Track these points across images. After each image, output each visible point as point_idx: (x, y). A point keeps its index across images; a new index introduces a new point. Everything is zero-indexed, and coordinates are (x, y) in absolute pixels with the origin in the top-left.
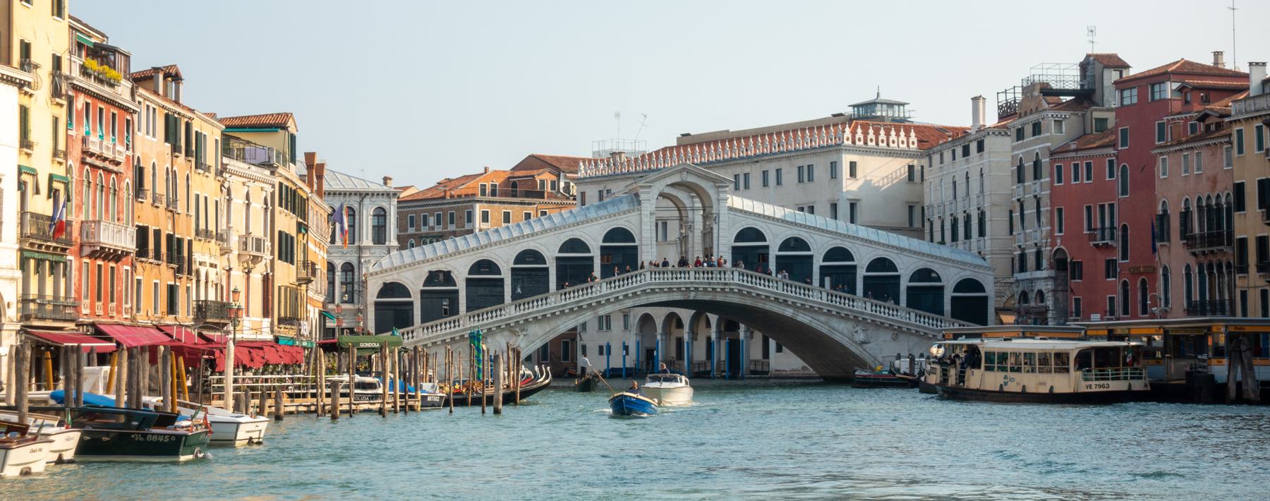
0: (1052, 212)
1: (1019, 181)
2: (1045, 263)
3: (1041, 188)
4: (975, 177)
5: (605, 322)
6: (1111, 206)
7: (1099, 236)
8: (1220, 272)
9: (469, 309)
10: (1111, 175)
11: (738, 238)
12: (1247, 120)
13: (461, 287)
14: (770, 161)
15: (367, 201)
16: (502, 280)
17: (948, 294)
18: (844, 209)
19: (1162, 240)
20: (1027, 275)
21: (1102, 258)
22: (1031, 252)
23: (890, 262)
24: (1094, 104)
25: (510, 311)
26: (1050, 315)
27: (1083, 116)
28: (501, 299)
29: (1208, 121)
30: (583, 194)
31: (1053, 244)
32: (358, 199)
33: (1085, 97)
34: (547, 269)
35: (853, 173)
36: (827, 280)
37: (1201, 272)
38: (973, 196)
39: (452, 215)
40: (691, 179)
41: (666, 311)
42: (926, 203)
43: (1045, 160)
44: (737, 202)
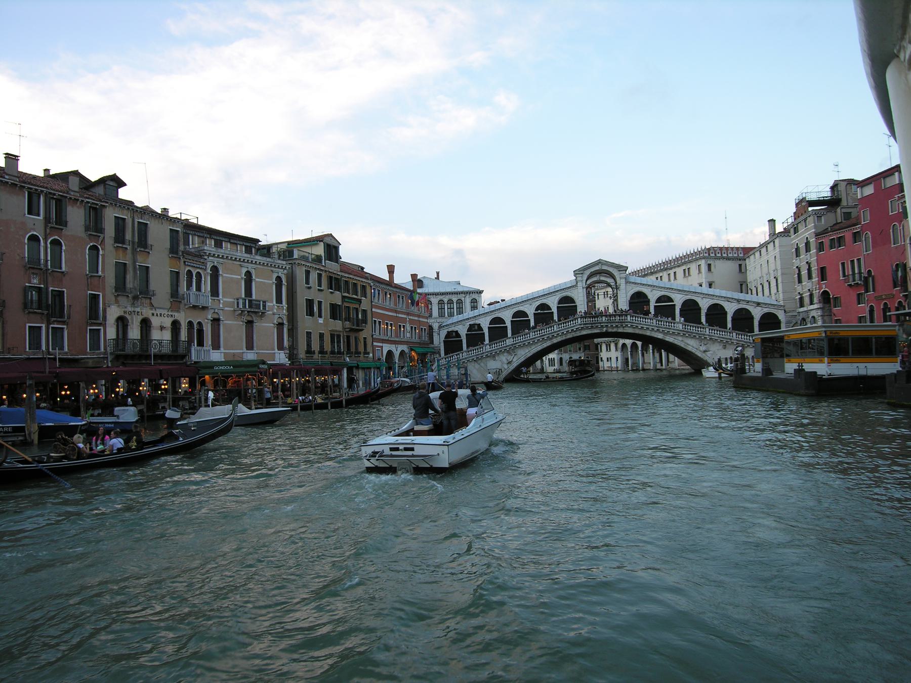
2: (815, 300)
5: (608, 348)
6: (859, 260)
7: (851, 279)
11: (633, 297)
13: (486, 331)
14: (671, 269)
22: (806, 295)
25: (509, 342)
27: (835, 212)
31: (820, 289)
40: (605, 268)
43: (812, 240)
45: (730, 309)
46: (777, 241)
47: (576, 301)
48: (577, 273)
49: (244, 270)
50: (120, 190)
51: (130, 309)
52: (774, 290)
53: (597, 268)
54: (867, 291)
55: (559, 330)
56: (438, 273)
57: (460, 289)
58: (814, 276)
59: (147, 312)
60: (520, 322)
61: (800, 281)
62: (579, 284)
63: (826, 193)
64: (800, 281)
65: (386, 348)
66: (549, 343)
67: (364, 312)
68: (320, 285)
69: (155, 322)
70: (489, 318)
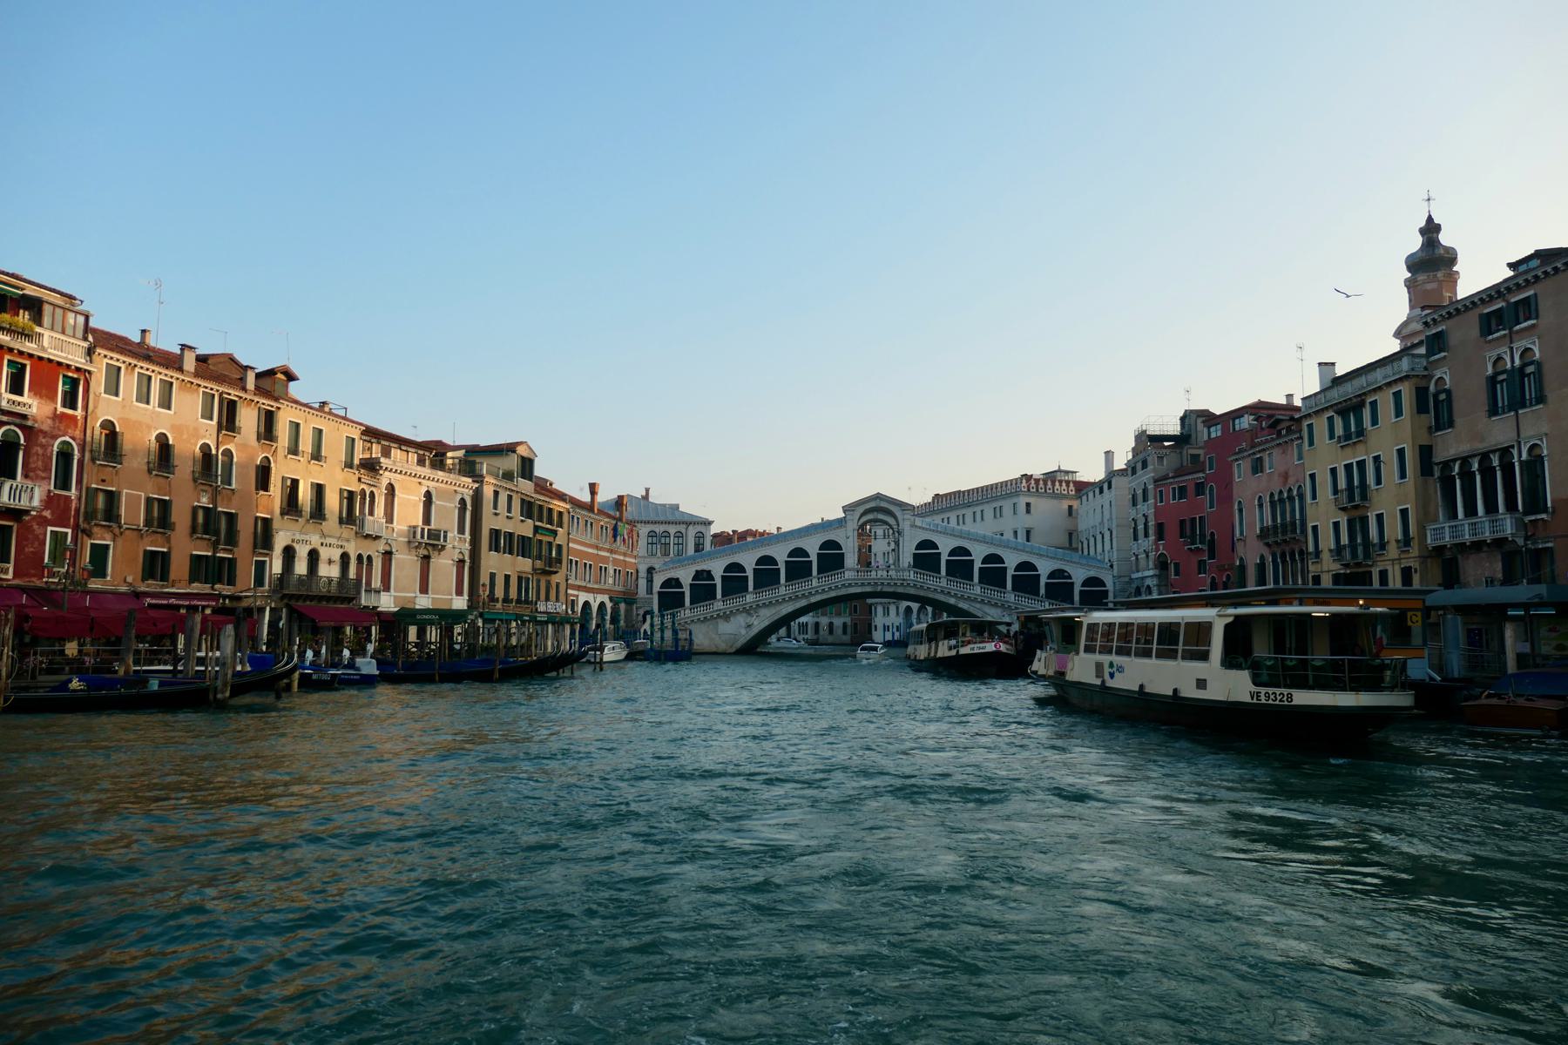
3: (1147, 508)
5: (886, 612)
9: (723, 595)
11: (919, 546)
12: (1317, 413)
13: (718, 582)
17: (1077, 589)
18: (1021, 538)
20: (1140, 575)
21: (1195, 559)
25: (750, 598)
28: (746, 589)
31: (1157, 549)
33: (1181, 440)
35: (1028, 511)
37: (1274, 561)
43: (1151, 487)
48: (846, 509)
49: (424, 489)
50: (292, 384)
51: (298, 537)
52: (1107, 547)
53: (872, 505)
55: (817, 586)
56: (647, 490)
57: (678, 518)
59: (315, 540)
60: (766, 574)
61: (1136, 539)
63: (1174, 428)
64: (1136, 539)
65: (583, 597)
66: (803, 603)
67: (559, 547)
68: (509, 510)
69: (324, 553)
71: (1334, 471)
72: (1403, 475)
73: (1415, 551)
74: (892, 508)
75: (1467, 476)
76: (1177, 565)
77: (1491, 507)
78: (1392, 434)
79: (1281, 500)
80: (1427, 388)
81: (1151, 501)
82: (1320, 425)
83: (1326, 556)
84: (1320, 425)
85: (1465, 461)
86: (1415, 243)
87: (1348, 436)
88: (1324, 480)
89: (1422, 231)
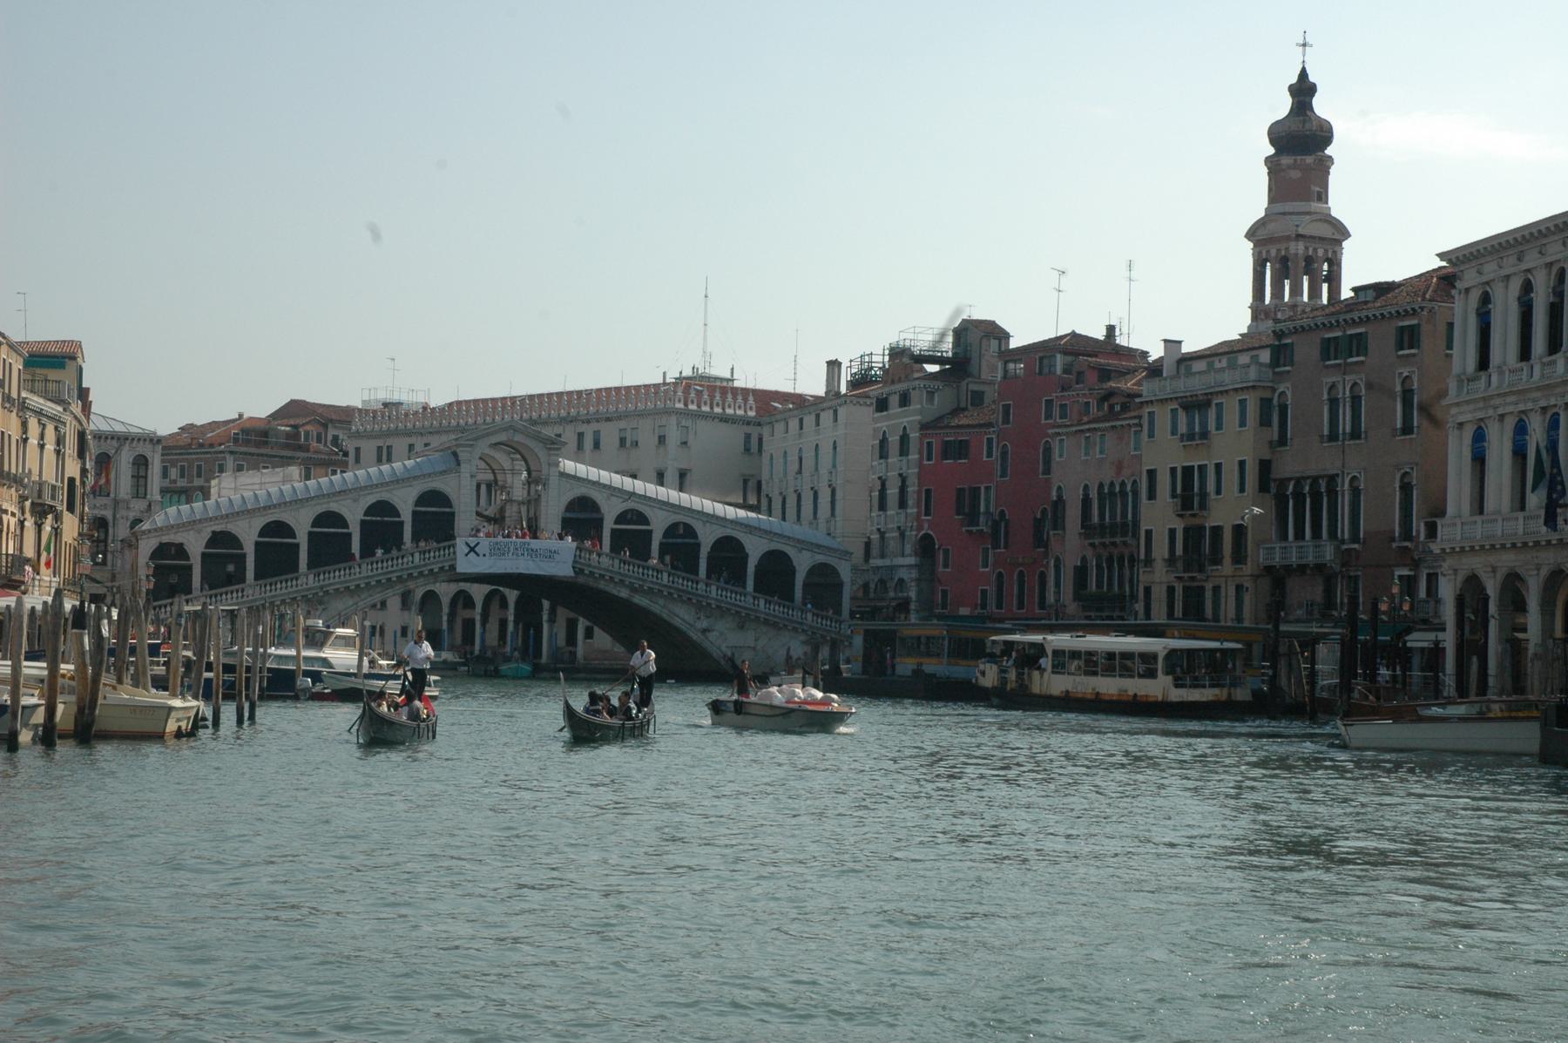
0: (919, 492)
1: (881, 457)
4: (826, 450)
6: (987, 488)
8: (1121, 567)
10: (990, 454)
14: (588, 422)
15: (127, 447)
16: (297, 545)
19: (1055, 528)
20: (887, 562)
23: (738, 541)
24: (969, 375)
25: (307, 580)
26: (912, 606)
28: (294, 567)
29: (1113, 400)
30: (358, 450)
31: (920, 528)
32: (115, 443)
34: (349, 535)
36: (668, 558)
37: (1099, 567)
38: (824, 471)
39: (199, 467)
40: (518, 438)
41: (453, 588)
42: (765, 477)
43: (914, 435)
44: (569, 466)
45: (755, 549)
46: (842, 411)
47: (455, 503)
53: (503, 437)
54: (996, 546)
58: (910, 502)
61: (882, 506)
62: (464, 468)
63: (947, 346)
64: (882, 506)
70: (259, 522)
71: (1173, 470)
72: (1242, 490)
73: (1248, 569)
74: (531, 444)
75: (1299, 497)
76: (946, 552)
77: (1317, 534)
78: (1235, 443)
79: (1112, 493)
80: (1270, 400)
81: (914, 456)
82: (1163, 416)
83: (1159, 566)
84: (1163, 416)
85: (1299, 482)
86: (1282, 106)
87: (1190, 436)
88: (1164, 481)
89: (1294, 90)
